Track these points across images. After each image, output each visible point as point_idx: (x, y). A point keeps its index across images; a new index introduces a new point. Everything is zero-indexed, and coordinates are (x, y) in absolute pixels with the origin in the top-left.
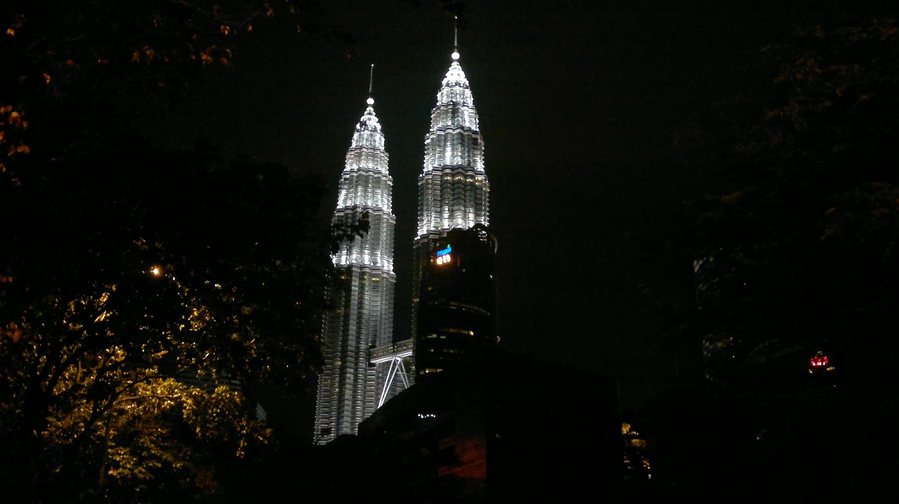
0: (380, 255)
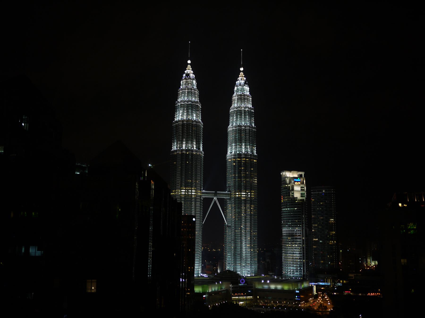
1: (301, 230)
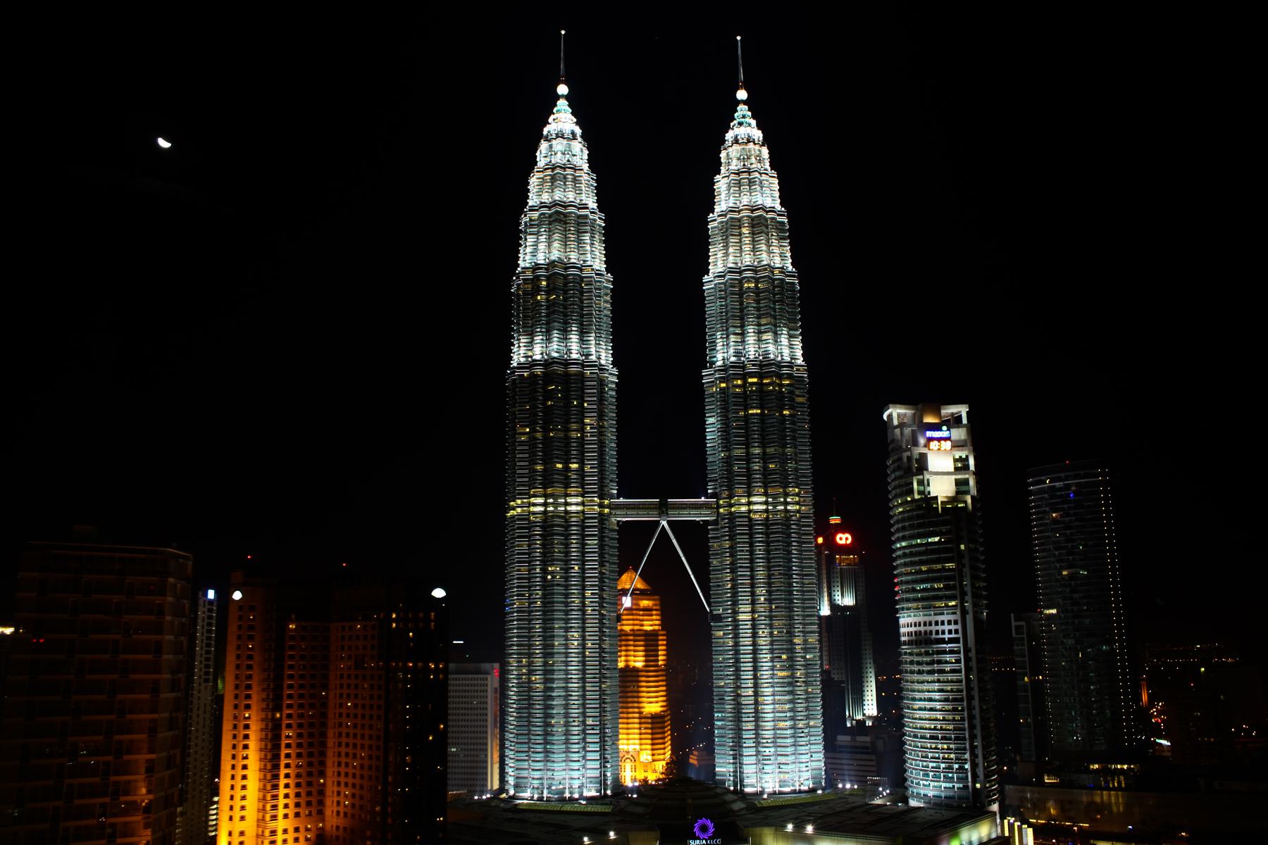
0: (593, 342)
1: (958, 617)
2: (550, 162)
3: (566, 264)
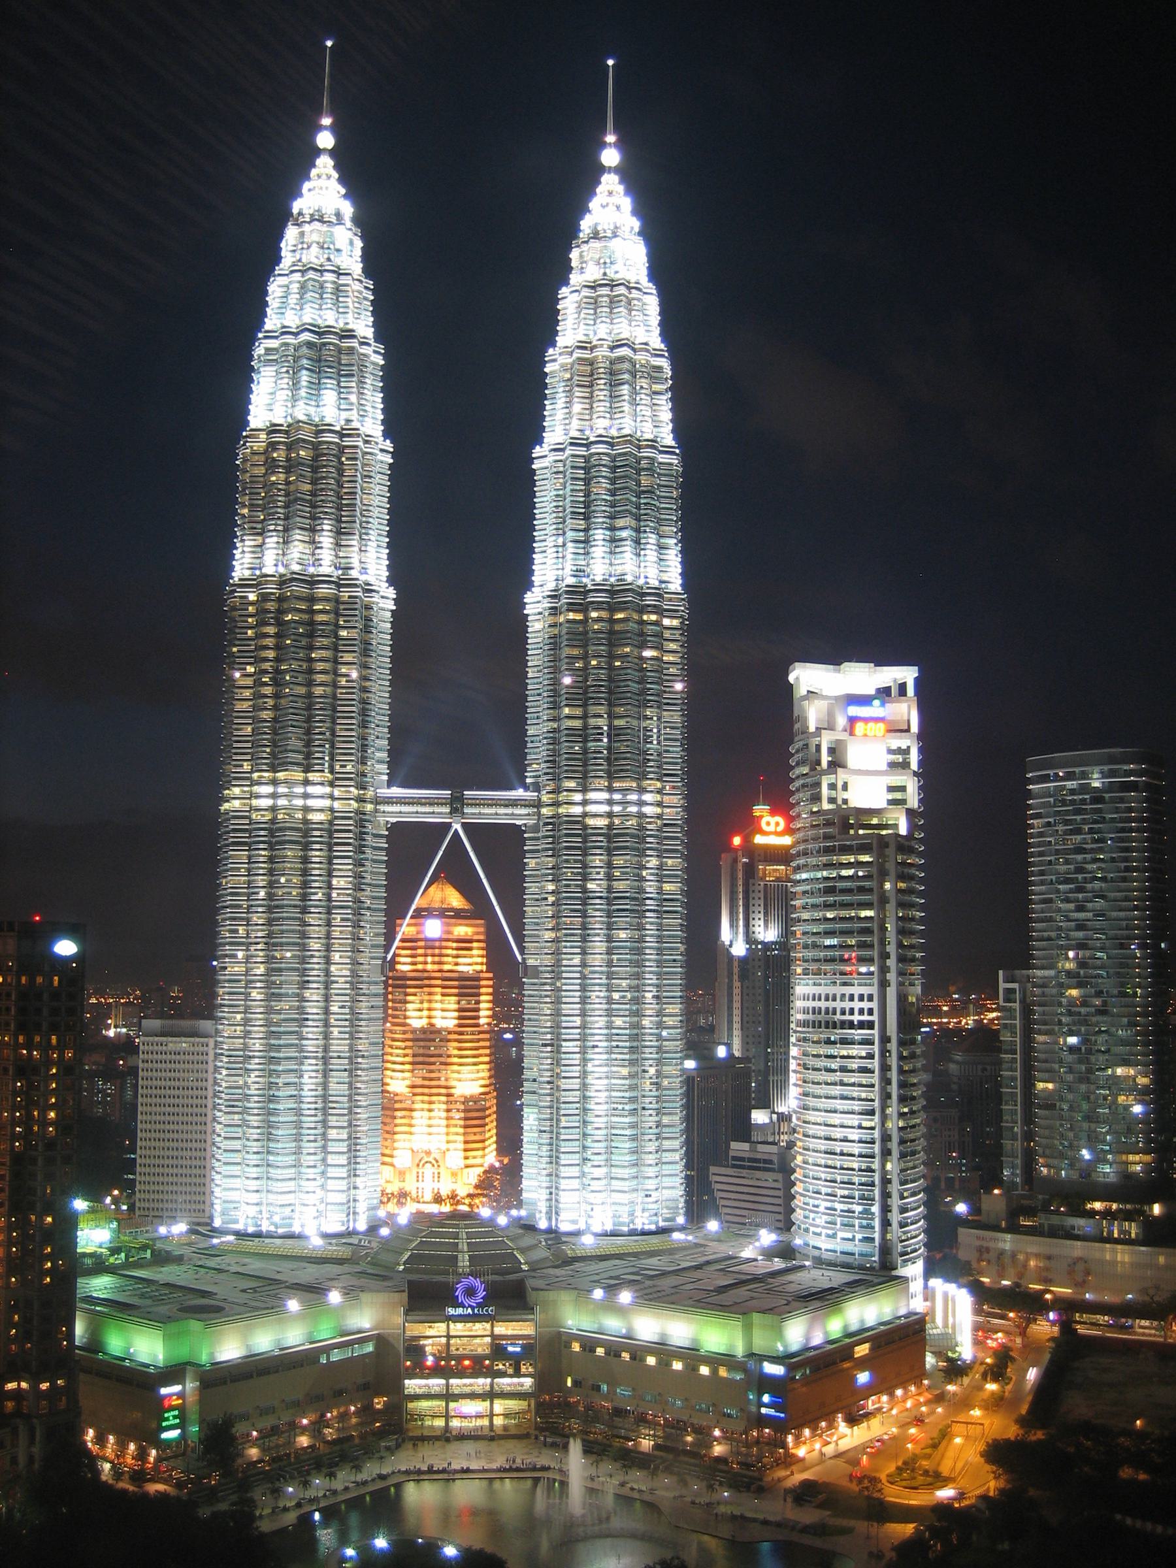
1: (874, 990)
2: (300, 260)
3: (316, 426)
